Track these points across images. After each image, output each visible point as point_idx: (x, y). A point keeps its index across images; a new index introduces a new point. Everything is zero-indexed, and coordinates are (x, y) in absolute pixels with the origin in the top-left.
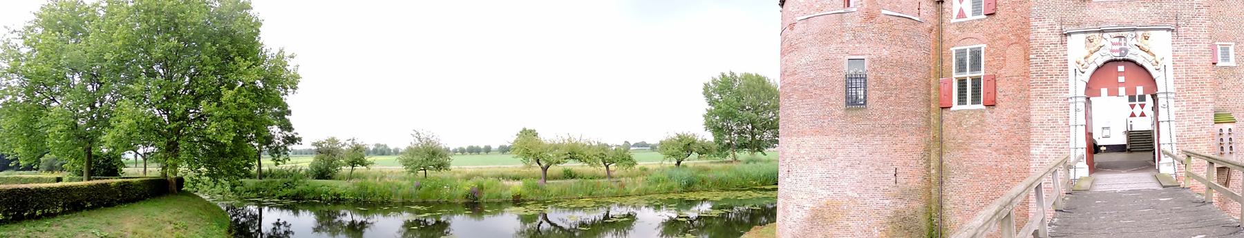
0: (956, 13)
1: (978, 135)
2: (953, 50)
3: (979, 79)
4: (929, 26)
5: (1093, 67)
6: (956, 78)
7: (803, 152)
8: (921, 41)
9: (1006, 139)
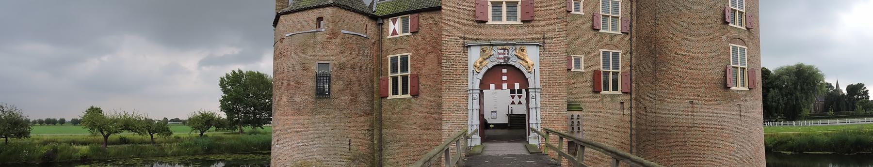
0: (391, 31)
1: (407, 116)
2: (389, 57)
3: (407, 76)
4: (373, 41)
5: (484, 70)
6: (391, 77)
7: (287, 127)
8: (367, 51)
9: (425, 118)
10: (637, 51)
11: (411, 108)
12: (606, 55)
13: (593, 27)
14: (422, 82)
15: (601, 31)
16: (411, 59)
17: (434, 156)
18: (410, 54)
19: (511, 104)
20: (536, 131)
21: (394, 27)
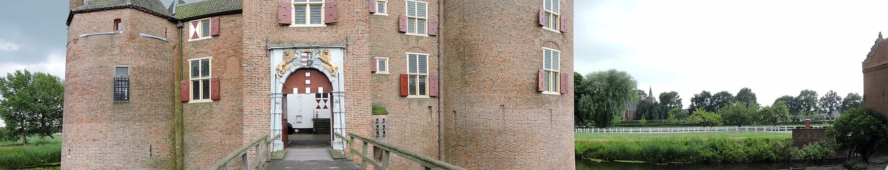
0: (191, 34)
1: (208, 121)
3: (208, 81)
4: (173, 44)
5: (287, 74)
6: (192, 81)
8: (167, 55)
9: (227, 123)
11: (212, 113)
12: (412, 58)
13: (399, 29)
15: (407, 33)
16: (212, 63)
18: (210, 58)
19: (317, 108)
20: (340, 136)
21: (194, 30)
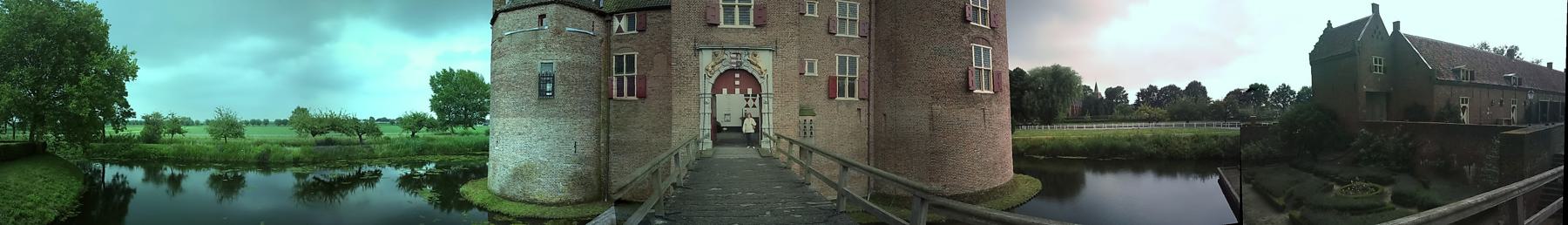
4: (600, 38)
7: (507, 128)
8: (594, 49)
10: (876, 55)
12: (842, 60)
14: (650, 83)
15: (837, 35)
17: (663, 160)
21: (620, 24)
